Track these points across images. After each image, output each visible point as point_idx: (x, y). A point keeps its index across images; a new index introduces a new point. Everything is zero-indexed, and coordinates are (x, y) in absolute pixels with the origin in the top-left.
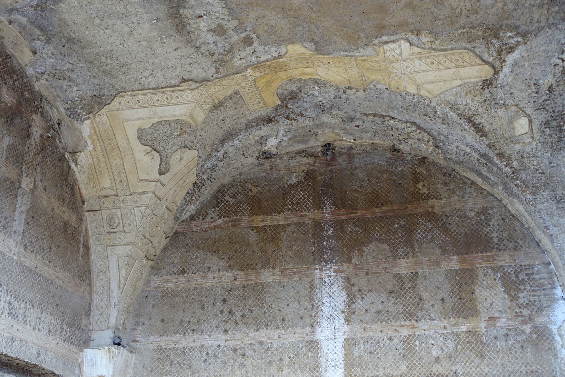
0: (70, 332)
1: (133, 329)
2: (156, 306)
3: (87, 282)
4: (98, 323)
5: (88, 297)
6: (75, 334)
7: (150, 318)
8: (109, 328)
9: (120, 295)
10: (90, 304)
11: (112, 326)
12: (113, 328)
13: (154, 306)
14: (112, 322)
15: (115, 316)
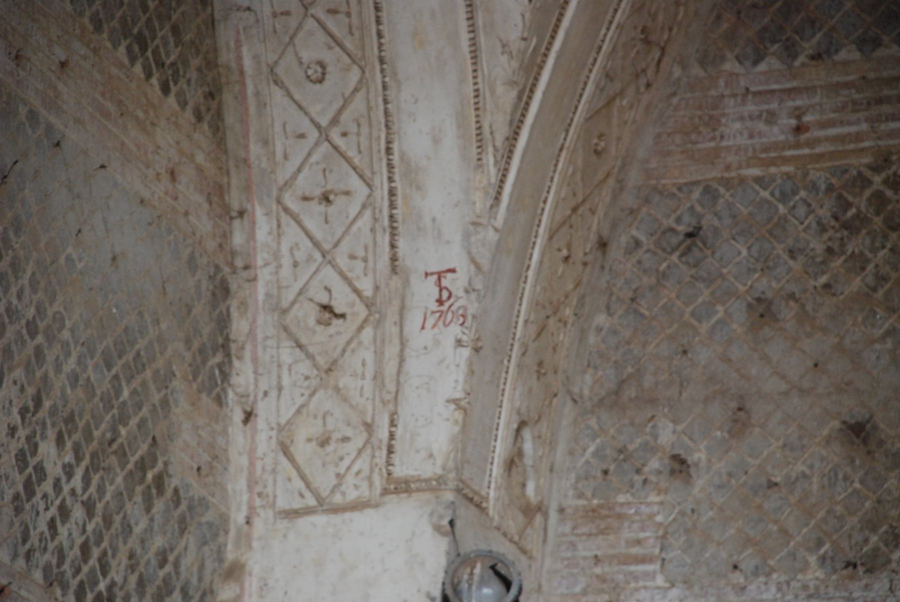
0: (89, 508)
1: (592, 514)
2: (788, 313)
3: (195, 96)
4: (303, 450)
5: (204, 225)
6: (127, 529)
7: (740, 420)
8: (401, 487)
9: (481, 202)
10: (222, 291)
11: (429, 470)
12: (434, 485)
13: (763, 311)
14: (430, 436)
15: (452, 381)
